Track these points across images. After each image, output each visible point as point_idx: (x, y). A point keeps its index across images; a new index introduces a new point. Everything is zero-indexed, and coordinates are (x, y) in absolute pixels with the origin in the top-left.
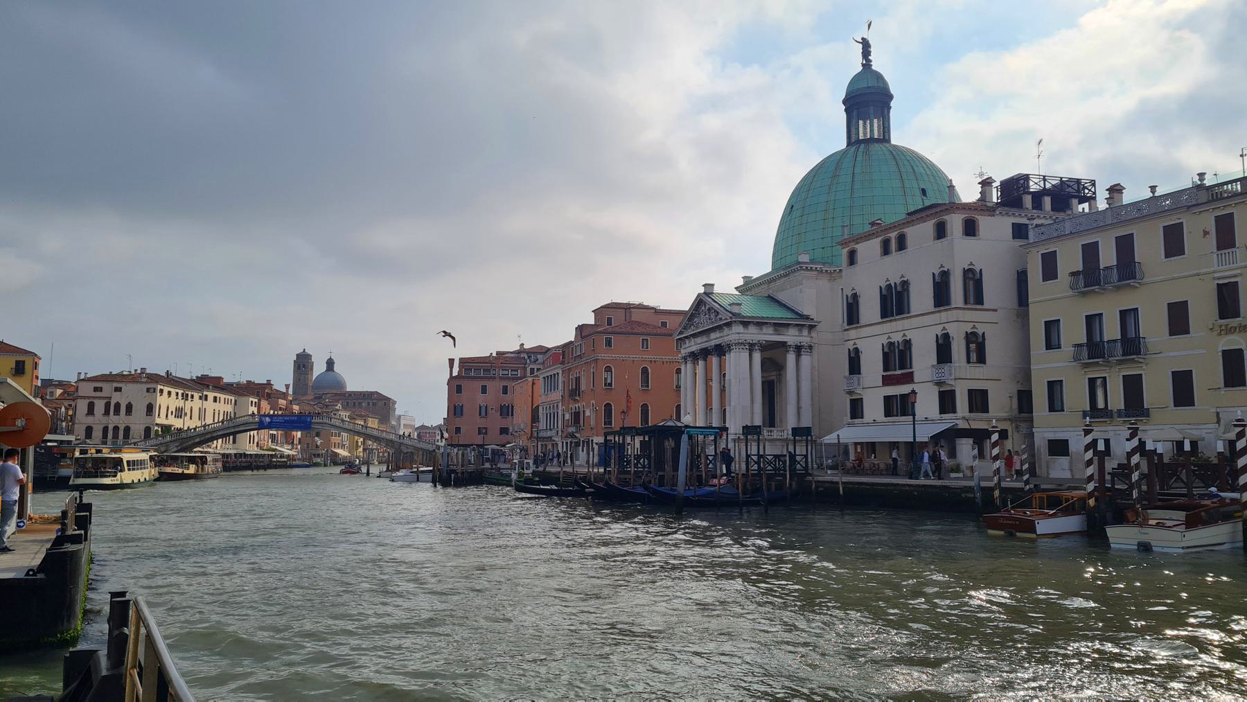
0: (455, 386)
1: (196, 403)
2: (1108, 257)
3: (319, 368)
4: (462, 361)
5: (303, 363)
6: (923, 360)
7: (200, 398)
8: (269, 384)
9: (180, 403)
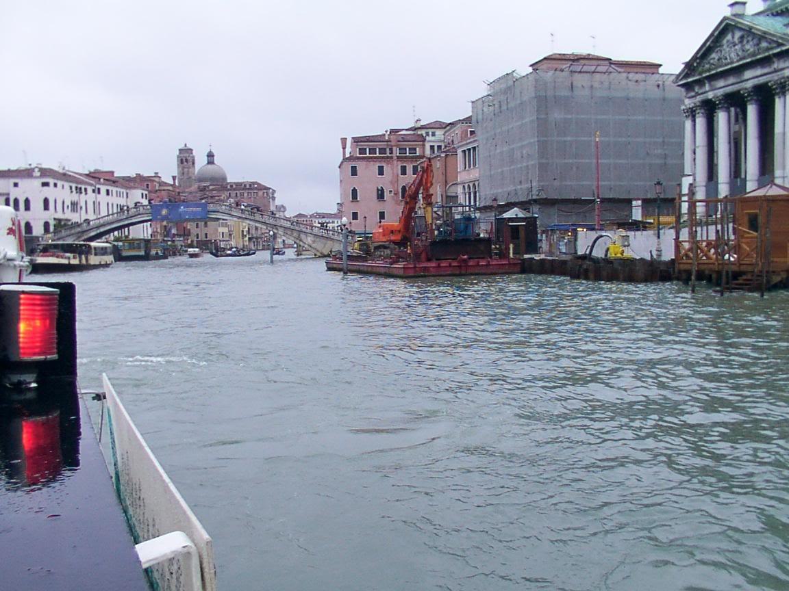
0: (351, 165)
1: (91, 197)
3: (201, 161)
4: (356, 140)
5: (185, 158)
7: (94, 191)
8: (157, 175)
9: (75, 197)
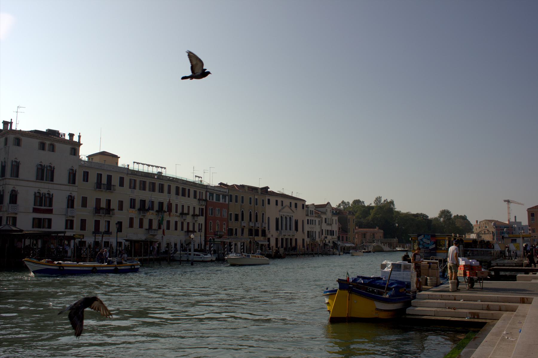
2: (104, 181)
6: (59, 203)
